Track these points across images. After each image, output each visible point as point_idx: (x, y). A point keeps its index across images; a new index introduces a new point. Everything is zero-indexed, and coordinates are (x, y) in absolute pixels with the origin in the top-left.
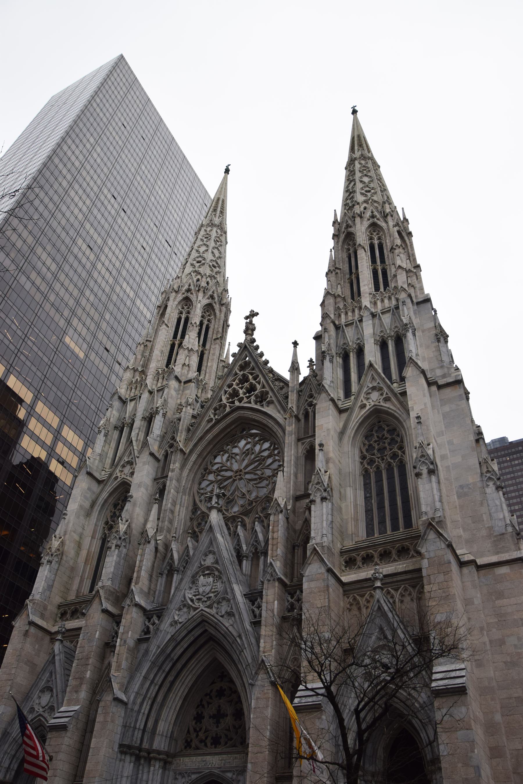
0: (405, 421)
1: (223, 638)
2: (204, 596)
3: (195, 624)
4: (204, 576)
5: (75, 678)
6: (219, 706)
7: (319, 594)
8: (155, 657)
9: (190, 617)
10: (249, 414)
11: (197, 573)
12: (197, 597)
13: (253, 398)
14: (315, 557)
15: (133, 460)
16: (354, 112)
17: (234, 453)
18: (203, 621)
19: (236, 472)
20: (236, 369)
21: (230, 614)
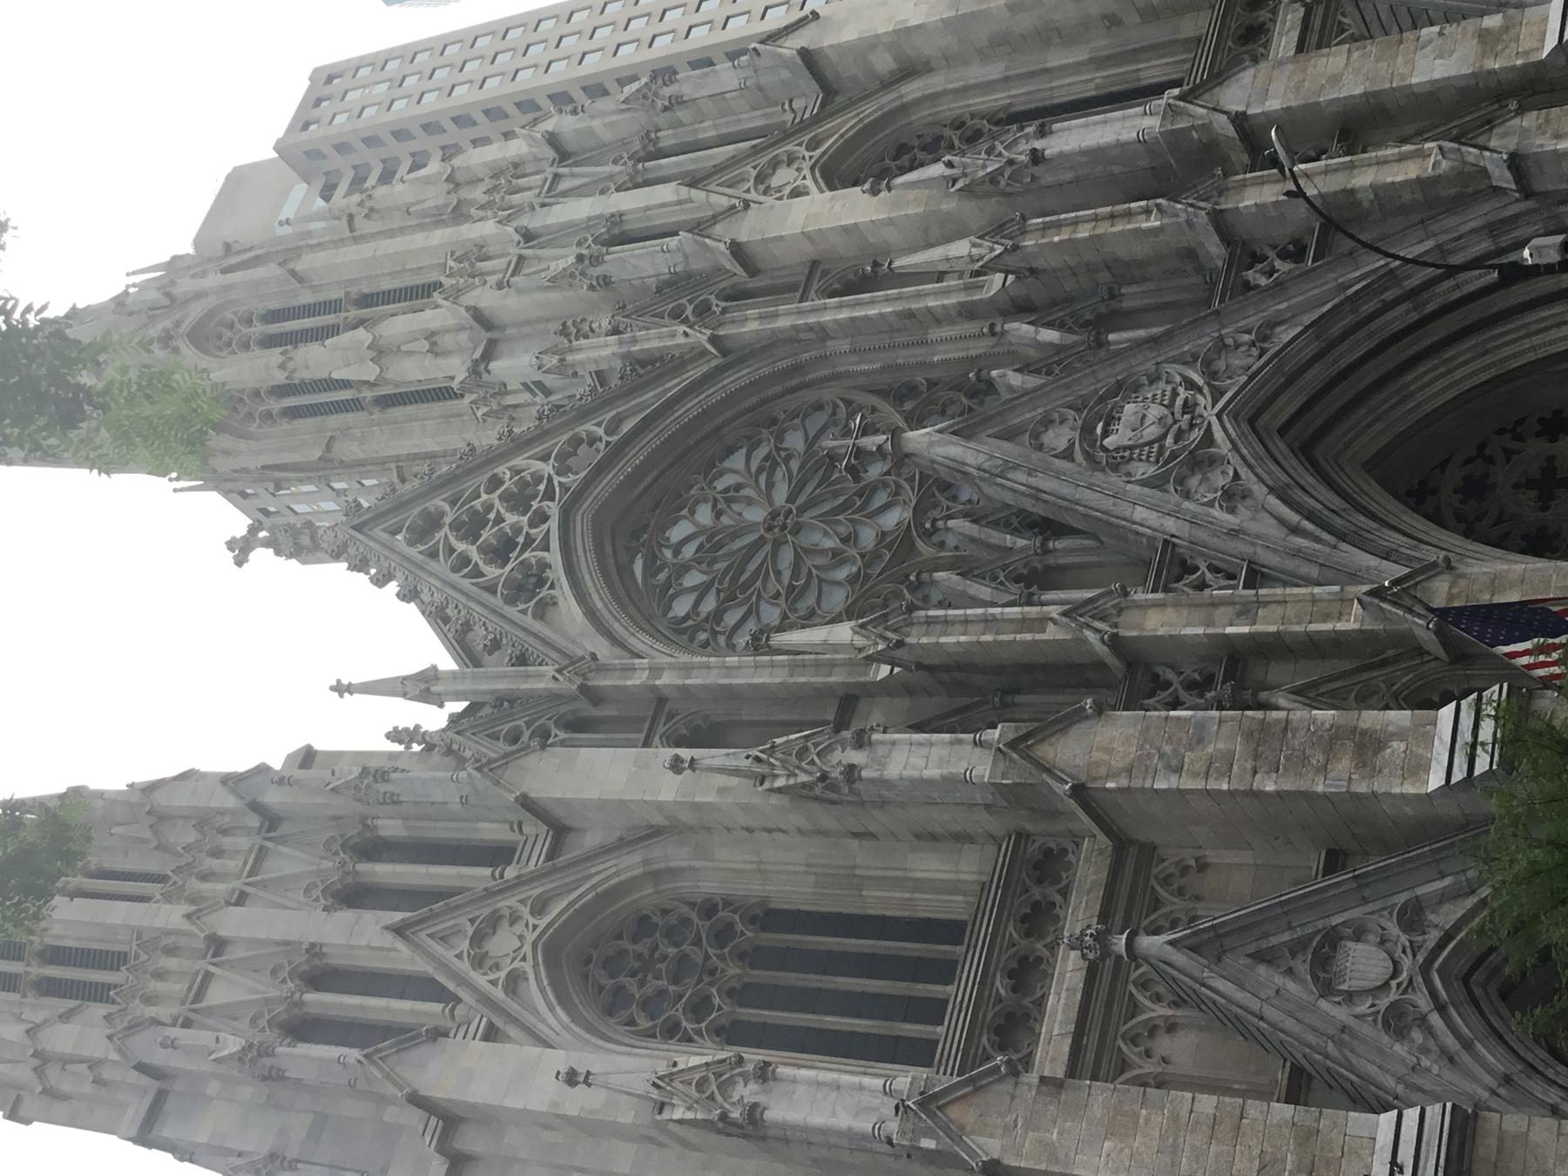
0: (901, 96)
1: (1329, 358)
2: (1175, 422)
3: (1252, 438)
4: (1106, 434)
5: (1323, 770)
6: (1516, 486)
7: (1310, 69)
8: (1325, 536)
9: (1230, 446)
10: (610, 480)
11: (1088, 456)
12: (1169, 440)
13: (556, 479)
14: (1207, 96)
17: (701, 547)
18: (1252, 422)
19: (769, 529)
20: (414, 552)
21: (1264, 334)
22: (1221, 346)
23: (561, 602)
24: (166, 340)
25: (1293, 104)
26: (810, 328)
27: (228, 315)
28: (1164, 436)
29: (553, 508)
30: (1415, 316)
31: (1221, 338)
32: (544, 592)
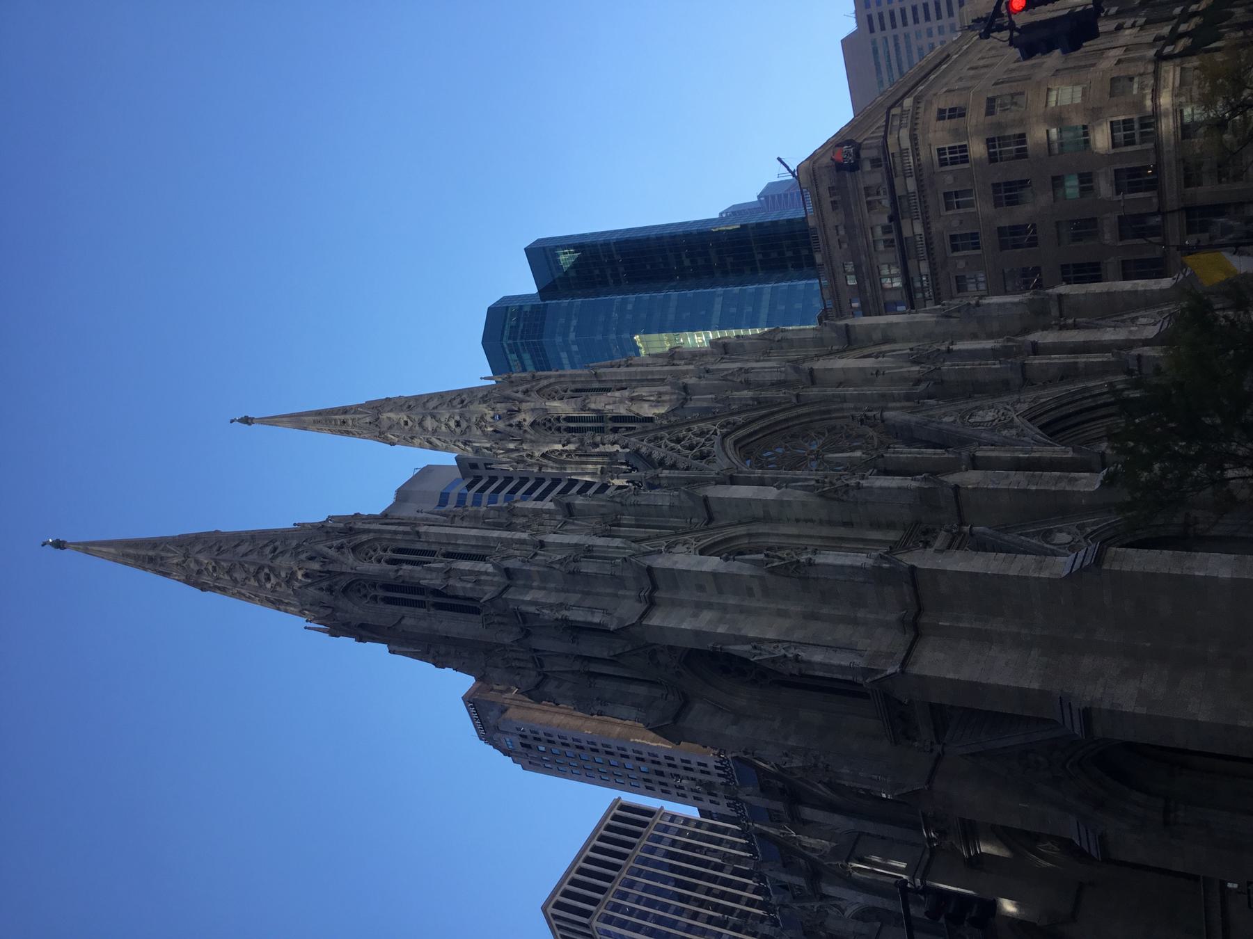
4: (969, 419)
15: (673, 540)
16: (247, 421)
22: (1019, 401)
23: (719, 461)
24: (526, 392)
25: (1056, 341)
26: (839, 396)
27: (557, 387)
28: (994, 420)
29: (717, 439)
30: (1093, 404)
31: (1019, 399)
32: (710, 458)
